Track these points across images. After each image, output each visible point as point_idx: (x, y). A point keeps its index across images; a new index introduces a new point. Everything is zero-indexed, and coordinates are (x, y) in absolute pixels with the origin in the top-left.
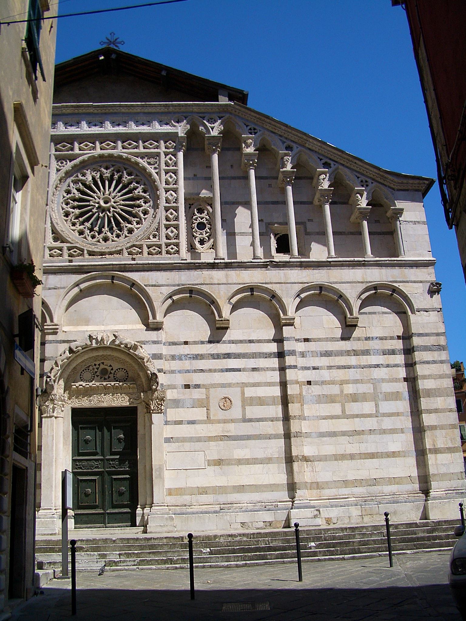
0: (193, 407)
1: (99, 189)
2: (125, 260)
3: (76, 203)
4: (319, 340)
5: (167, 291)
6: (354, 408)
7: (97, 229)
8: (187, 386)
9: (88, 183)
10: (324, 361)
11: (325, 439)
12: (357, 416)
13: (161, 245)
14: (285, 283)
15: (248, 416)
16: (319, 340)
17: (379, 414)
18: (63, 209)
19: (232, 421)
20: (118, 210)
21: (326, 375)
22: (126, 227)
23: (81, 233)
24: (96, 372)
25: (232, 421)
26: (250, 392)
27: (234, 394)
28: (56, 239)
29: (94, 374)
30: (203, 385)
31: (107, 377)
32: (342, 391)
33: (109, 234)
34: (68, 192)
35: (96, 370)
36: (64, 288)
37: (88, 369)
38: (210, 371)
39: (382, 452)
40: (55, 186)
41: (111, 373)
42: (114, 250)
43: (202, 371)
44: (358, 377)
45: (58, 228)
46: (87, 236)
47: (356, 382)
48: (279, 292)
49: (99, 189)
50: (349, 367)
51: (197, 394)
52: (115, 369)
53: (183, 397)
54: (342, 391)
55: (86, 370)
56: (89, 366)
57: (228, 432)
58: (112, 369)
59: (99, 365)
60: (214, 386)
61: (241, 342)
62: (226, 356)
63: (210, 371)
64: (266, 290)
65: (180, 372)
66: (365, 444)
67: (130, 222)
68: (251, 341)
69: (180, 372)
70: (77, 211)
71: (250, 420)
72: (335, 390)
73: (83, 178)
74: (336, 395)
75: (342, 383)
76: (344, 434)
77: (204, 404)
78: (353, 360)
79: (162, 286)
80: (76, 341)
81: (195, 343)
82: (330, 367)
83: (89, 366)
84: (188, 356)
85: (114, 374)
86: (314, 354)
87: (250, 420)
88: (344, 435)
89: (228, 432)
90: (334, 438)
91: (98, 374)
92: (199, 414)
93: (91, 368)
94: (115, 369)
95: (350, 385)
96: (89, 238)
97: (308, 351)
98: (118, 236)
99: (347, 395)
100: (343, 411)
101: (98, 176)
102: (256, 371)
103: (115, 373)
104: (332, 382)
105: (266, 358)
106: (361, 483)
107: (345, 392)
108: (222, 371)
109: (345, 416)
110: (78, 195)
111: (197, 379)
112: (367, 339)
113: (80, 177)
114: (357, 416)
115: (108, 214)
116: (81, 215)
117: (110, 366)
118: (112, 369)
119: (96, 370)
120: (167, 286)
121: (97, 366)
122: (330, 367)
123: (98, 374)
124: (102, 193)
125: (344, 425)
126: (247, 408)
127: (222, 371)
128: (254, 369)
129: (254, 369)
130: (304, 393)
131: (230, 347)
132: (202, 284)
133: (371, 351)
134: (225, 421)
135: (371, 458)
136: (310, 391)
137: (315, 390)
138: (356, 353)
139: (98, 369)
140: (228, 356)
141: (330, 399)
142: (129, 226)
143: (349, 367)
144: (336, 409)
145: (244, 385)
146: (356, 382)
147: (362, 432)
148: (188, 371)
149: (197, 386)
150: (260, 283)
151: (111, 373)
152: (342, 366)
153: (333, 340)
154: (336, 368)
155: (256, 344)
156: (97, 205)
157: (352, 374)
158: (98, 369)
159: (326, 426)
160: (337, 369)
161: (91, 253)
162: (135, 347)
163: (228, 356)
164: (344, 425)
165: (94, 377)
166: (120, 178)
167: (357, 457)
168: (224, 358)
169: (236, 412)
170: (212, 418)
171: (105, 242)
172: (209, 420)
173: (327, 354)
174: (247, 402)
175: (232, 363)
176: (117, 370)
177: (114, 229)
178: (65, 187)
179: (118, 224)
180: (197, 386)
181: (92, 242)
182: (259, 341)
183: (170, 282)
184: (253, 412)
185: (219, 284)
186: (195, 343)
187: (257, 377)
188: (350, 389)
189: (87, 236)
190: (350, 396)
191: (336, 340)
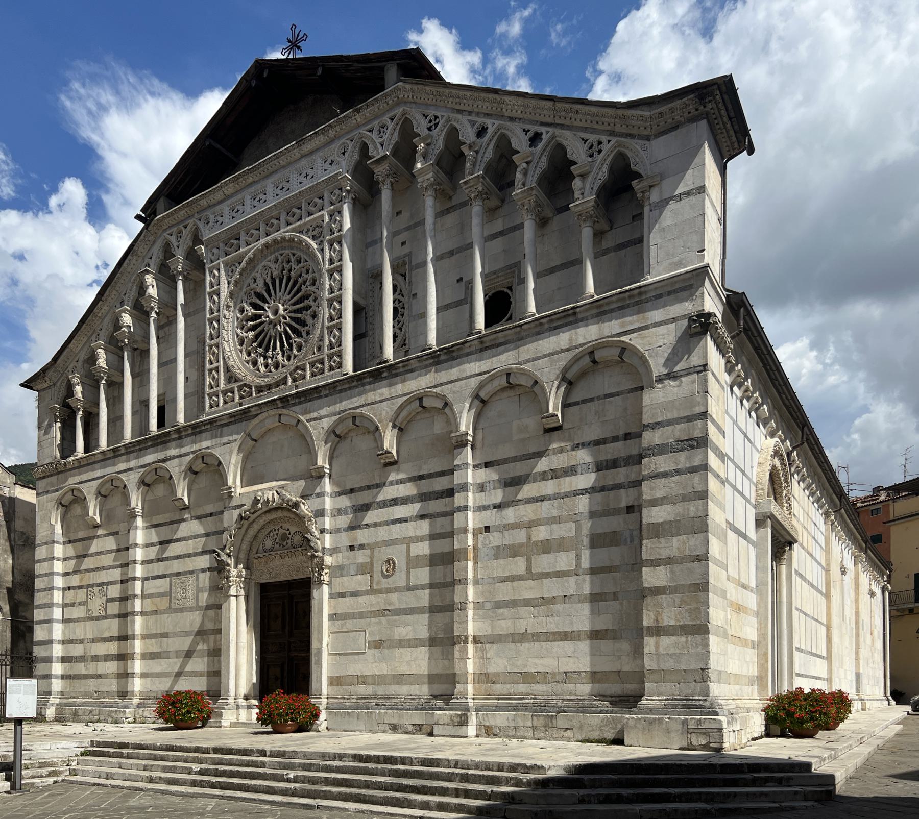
2: (290, 390)
5: (326, 423)
6: (544, 563)
8: (352, 548)
12: (547, 575)
13: (323, 359)
15: (413, 582)
17: (581, 571)
18: (238, 335)
23: (255, 363)
30: (368, 545)
31: (285, 544)
32: (529, 538)
34: (242, 311)
35: (276, 536)
39: (579, 631)
41: (288, 539)
44: (555, 513)
45: (231, 363)
48: (450, 397)
51: (361, 557)
54: (529, 538)
56: (269, 533)
58: (290, 534)
59: (278, 530)
60: (378, 544)
62: (393, 502)
64: (436, 395)
66: (556, 618)
70: (251, 334)
72: (520, 536)
74: (521, 545)
75: (531, 525)
76: (527, 602)
81: (361, 489)
83: (269, 533)
88: (527, 605)
91: (277, 541)
93: (271, 534)
95: (542, 528)
97: (489, 481)
100: (529, 568)
104: (515, 526)
106: (546, 677)
107: (533, 539)
109: (530, 575)
114: (547, 575)
116: (256, 337)
118: (290, 534)
121: (277, 532)
123: (277, 541)
125: (529, 590)
130: (479, 546)
131: (398, 490)
132: (363, 406)
135: (562, 640)
137: (495, 539)
139: (277, 534)
141: (513, 551)
144: (519, 566)
147: (552, 600)
149: (362, 547)
150: (428, 388)
151: (288, 539)
152: (533, 498)
153: (523, 458)
154: (524, 502)
155: (427, 480)
158: (277, 534)
160: (526, 503)
161: (260, 389)
162: (296, 505)
164: (529, 590)
167: (542, 638)
168: (391, 506)
179: (288, 338)
180: (362, 547)
182: (431, 476)
185: (381, 401)
186: (361, 489)
188: (541, 533)
190: (539, 544)
191: (528, 457)
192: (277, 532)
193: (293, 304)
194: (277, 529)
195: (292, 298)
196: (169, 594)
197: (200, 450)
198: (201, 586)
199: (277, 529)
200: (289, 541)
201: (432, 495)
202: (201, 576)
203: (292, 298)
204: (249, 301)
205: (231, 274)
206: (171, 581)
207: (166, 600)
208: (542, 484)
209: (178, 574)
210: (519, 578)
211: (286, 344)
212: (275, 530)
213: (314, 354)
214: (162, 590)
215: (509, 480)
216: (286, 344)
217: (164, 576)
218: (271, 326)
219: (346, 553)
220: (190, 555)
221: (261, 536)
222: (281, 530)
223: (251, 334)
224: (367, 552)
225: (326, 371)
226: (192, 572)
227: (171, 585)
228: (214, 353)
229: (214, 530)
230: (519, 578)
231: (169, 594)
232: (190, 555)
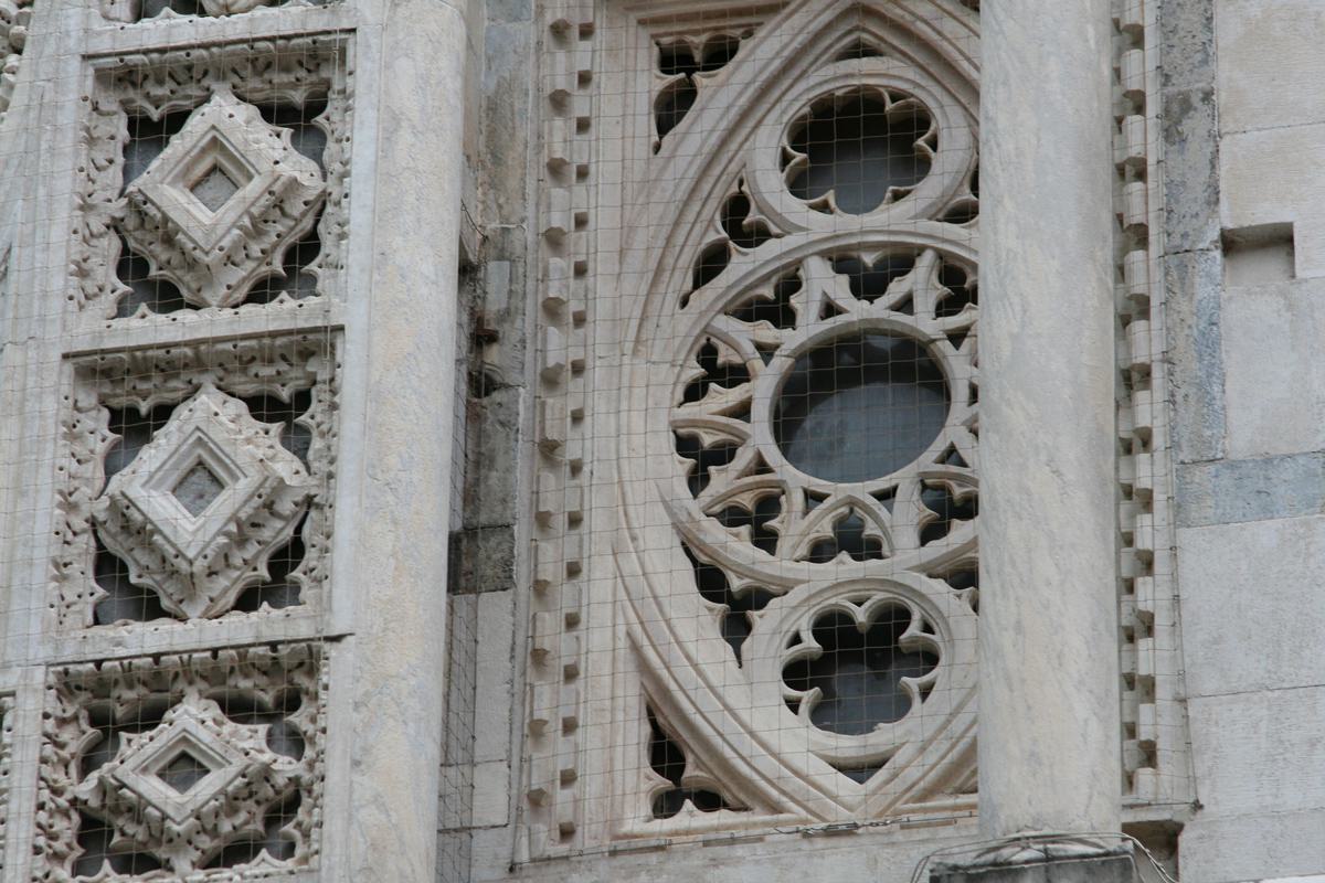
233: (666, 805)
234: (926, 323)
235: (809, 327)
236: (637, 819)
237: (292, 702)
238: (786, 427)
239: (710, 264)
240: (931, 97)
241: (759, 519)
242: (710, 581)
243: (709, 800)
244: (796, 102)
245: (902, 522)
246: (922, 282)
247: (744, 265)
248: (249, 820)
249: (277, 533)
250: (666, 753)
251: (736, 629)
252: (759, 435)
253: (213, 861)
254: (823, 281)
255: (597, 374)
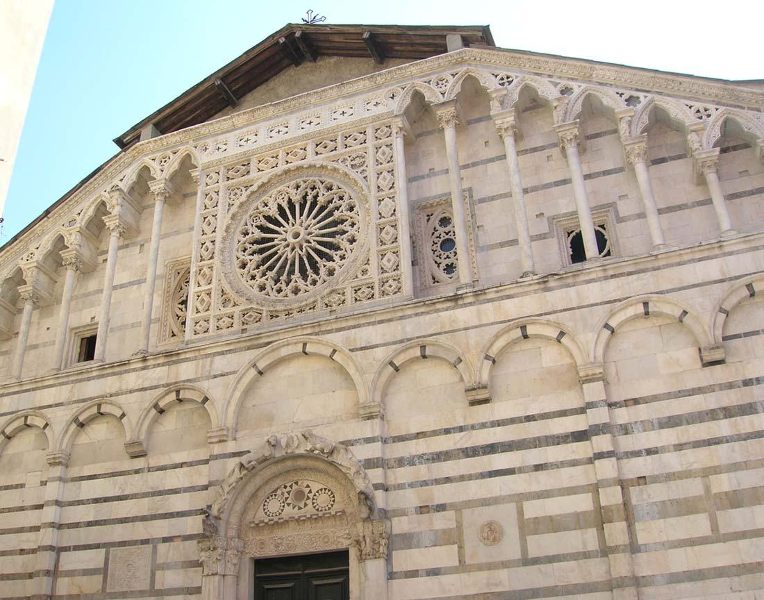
0: (436, 546)
1: (287, 220)
3: (256, 247)
4: (655, 398)
7: (284, 278)
9: (271, 215)
10: (668, 437)
11: (683, 585)
12: (743, 535)
14: (579, 308)
15: (533, 553)
16: (655, 398)
19: (505, 565)
20: (314, 244)
21: (673, 462)
22: (325, 266)
24: (287, 499)
25: (505, 565)
26: (533, 509)
27: (505, 515)
28: (225, 303)
29: (283, 502)
32: (707, 489)
33: (301, 283)
35: (286, 495)
36: (234, 372)
37: (275, 495)
38: (462, 478)
40: (224, 228)
41: (308, 498)
42: (304, 303)
43: (448, 480)
44: (738, 458)
46: (270, 291)
47: (735, 467)
49: (287, 220)
50: (717, 441)
51: (442, 521)
52: (314, 492)
53: (417, 530)
54: (707, 489)
55: (272, 496)
56: (276, 490)
57: (497, 585)
58: (310, 492)
59: (291, 486)
60: (470, 504)
61: (512, 421)
62: (488, 450)
63: (462, 478)
65: (411, 485)
67: (331, 259)
68: (529, 419)
69: (411, 485)
70: (257, 258)
71: (536, 561)
72: (694, 488)
73: (266, 208)
75: (708, 472)
76: (720, 572)
77: (452, 537)
78: (723, 427)
79: (377, 346)
80: (249, 452)
82: (679, 447)
83: (276, 490)
84: (425, 457)
85: (313, 499)
86: (648, 426)
87: (536, 561)
89: (497, 585)
90: (700, 584)
91: (288, 501)
92: (445, 556)
93: (279, 492)
94: (314, 492)
95: (724, 476)
96: (273, 294)
97: (636, 422)
98: (314, 282)
99: (718, 495)
100: (714, 526)
101: (286, 202)
102: (542, 469)
103: (315, 497)
105: (558, 444)
107: (714, 491)
108: (483, 476)
109: (717, 537)
110: (258, 234)
111: (442, 494)
112: (747, 383)
113: (261, 209)
114: (743, 535)
115: (300, 252)
116: (264, 261)
117: (308, 486)
118: (310, 492)
119: (286, 495)
120: (384, 345)
122: (679, 447)
123: (288, 501)
124: (290, 224)
125: (719, 555)
126: (528, 538)
127: (483, 476)
128: (538, 467)
129: (538, 467)
131: (494, 433)
133: (759, 404)
134: (491, 566)
136: (645, 496)
137: (657, 493)
138: (728, 412)
139: (289, 493)
140: (491, 449)
141: (686, 507)
142: (330, 264)
143: (717, 441)
144: (699, 525)
145: (520, 498)
146: (735, 467)
148: (425, 483)
149: (441, 508)
151: (308, 498)
152: (704, 441)
153: (680, 395)
155: (539, 422)
156: (284, 243)
157: (722, 454)
158: (289, 493)
159: (681, 560)
163: (491, 449)
164: (719, 555)
165: (283, 506)
166: (316, 197)
168: (484, 454)
169: (510, 548)
170: (468, 561)
171: (296, 294)
172: (463, 566)
173: (672, 422)
174: (529, 527)
175: (500, 461)
176: (318, 492)
177: (308, 273)
178: (241, 228)
180: (441, 508)
181: (276, 298)
183: (389, 339)
184: (541, 544)
185: (466, 329)
187: (543, 481)
188: (723, 483)
189: (270, 291)
191: (687, 394)
192: (288, 489)
193: (321, 229)
194: (288, 485)
195: (318, 223)
196: (104, 571)
197: (176, 383)
198: (160, 560)
199: (288, 485)
200: (309, 502)
201: (550, 440)
202: (162, 547)
203: (318, 223)
204: (254, 224)
205: (232, 196)
206: (107, 553)
207: (99, 578)
208: (712, 424)
209: (123, 544)
210: (703, 541)
211: (308, 268)
212: (285, 487)
213: (357, 277)
214: (91, 566)
215: (665, 420)
216: (308, 268)
217: (98, 546)
218: (289, 249)
219: (415, 516)
220: (144, 519)
221: (262, 495)
222: (295, 487)
223: (257, 258)
224: (450, 514)
225: (376, 295)
226: (145, 542)
227: (107, 560)
228: (204, 275)
229: (187, 485)
230: (703, 541)
231: (104, 571)
232: (144, 519)
233: (434, 283)
234: (452, 237)
235: (442, 239)
236: (432, 284)
237: (399, 279)
238: (441, 249)
239: (433, 233)
240: (450, 216)
241: (439, 256)
242: (436, 262)
243: (438, 282)
244: (439, 218)
245: (452, 256)
246: (451, 233)
247: (437, 234)
248: (396, 290)
249: (397, 264)
250: (434, 278)
251: (439, 266)
252: (439, 249)
253: (394, 294)
254: (443, 234)
255: (424, 245)
